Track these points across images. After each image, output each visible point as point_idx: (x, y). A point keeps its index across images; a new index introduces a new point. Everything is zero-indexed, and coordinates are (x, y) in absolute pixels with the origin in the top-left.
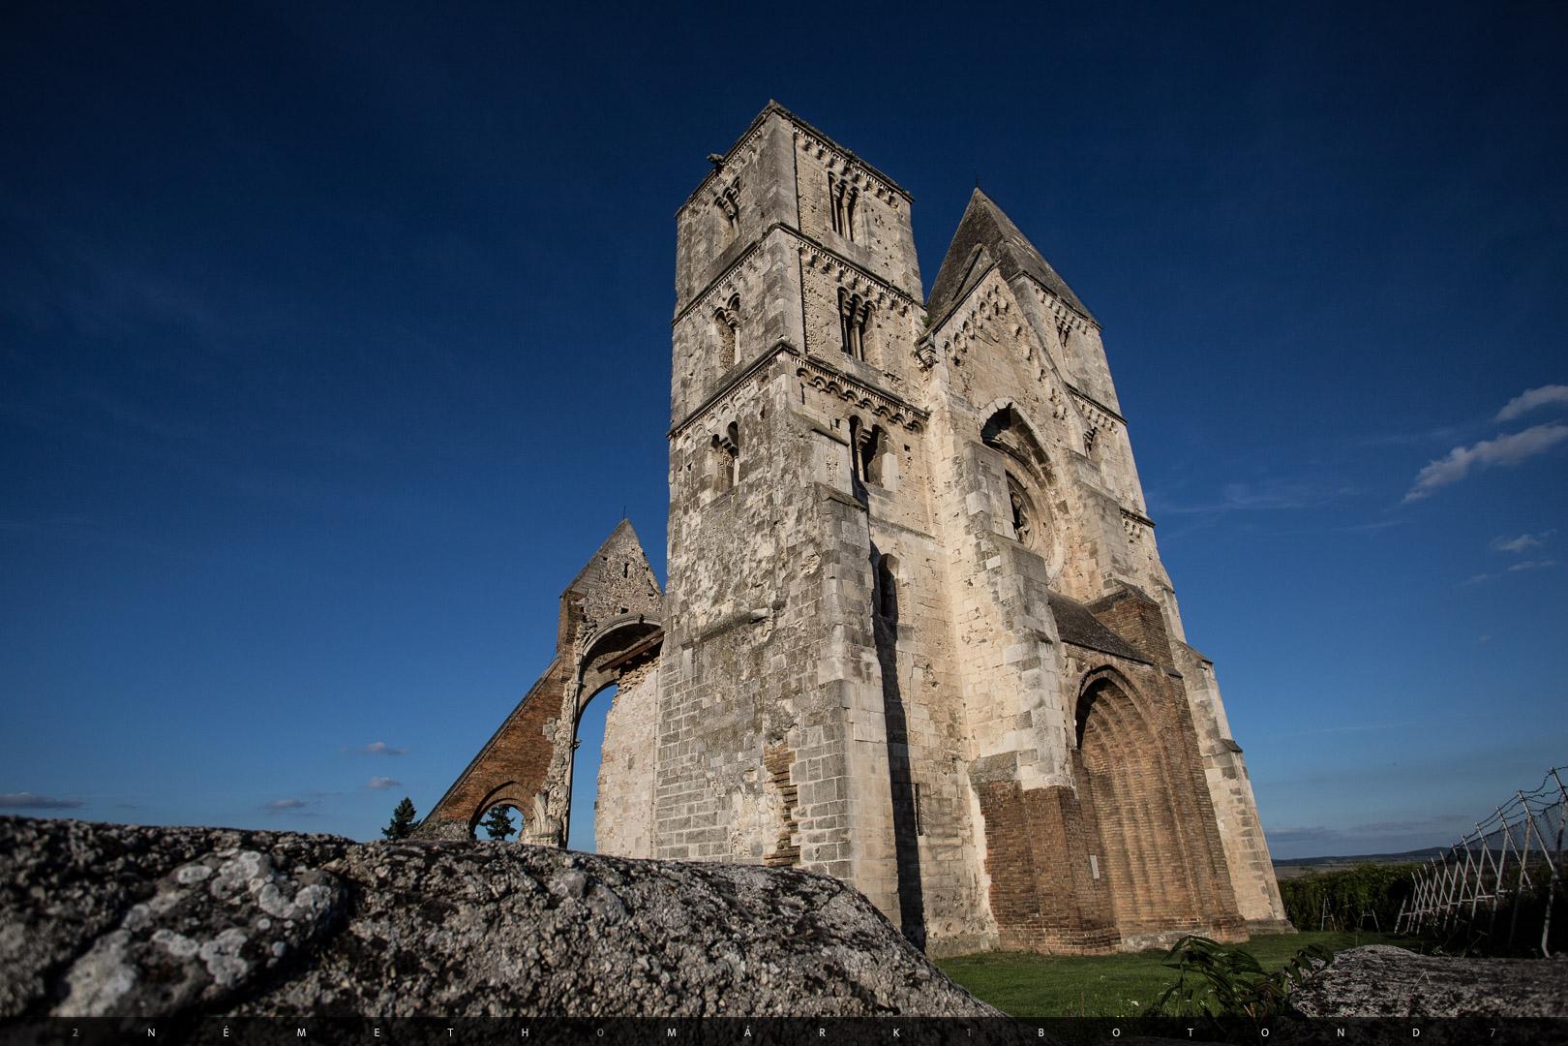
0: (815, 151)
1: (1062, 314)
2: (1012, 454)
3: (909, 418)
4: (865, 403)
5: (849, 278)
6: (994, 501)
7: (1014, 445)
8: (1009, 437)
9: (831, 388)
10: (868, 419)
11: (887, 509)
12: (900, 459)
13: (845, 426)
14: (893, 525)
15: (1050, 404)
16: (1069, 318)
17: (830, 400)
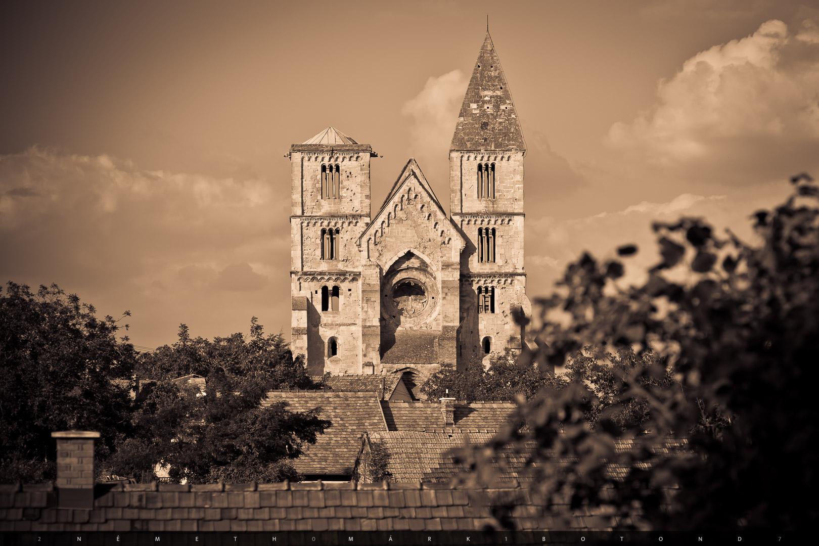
0: (313, 158)
1: (486, 158)
2: (416, 269)
3: (351, 278)
4: (329, 279)
5: (326, 223)
6: (370, 312)
7: (417, 265)
8: (414, 263)
9: (313, 279)
10: (330, 285)
11: (335, 319)
12: (345, 297)
13: (320, 292)
14: (337, 325)
15: (440, 239)
16: (492, 158)
17: (313, 284)
